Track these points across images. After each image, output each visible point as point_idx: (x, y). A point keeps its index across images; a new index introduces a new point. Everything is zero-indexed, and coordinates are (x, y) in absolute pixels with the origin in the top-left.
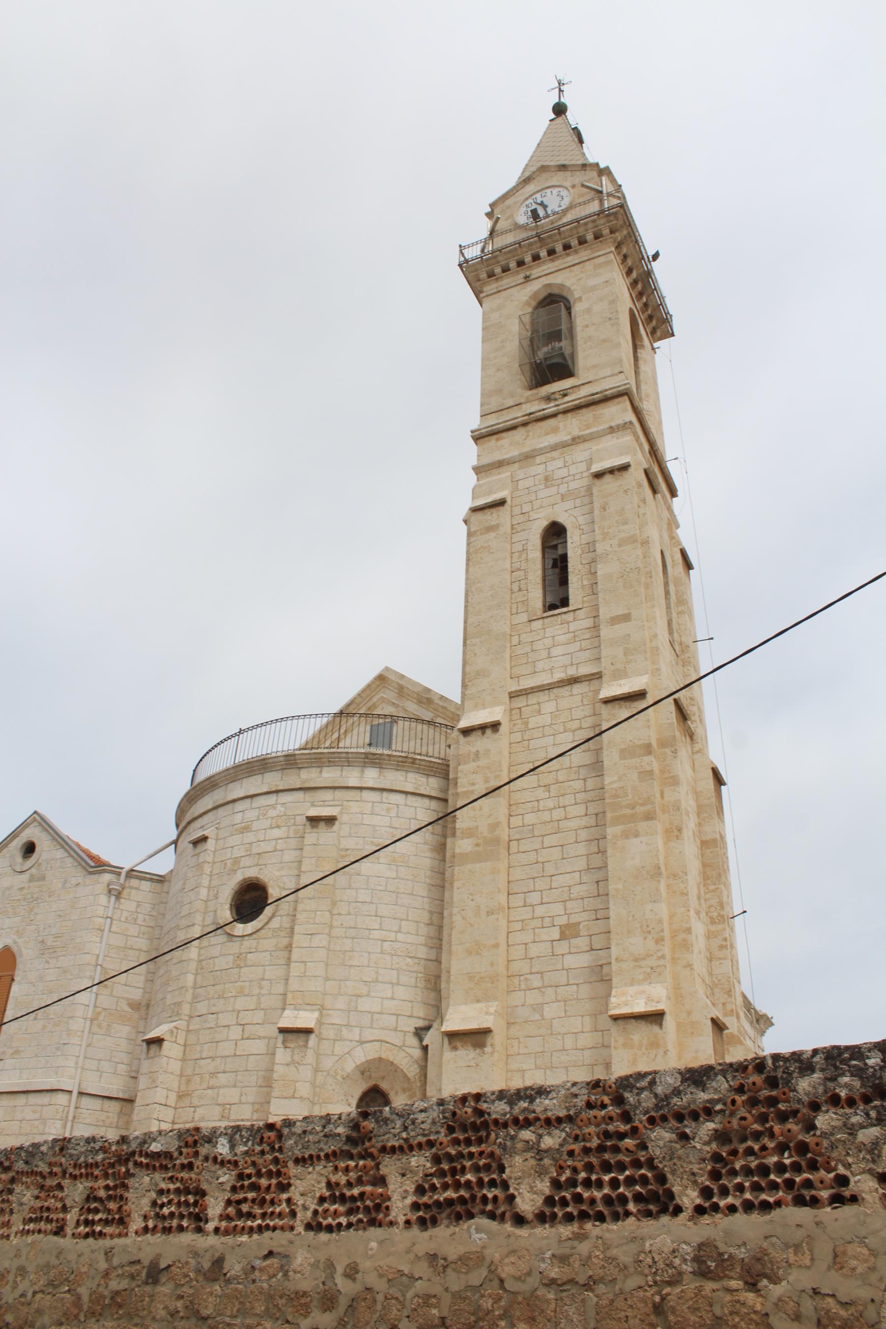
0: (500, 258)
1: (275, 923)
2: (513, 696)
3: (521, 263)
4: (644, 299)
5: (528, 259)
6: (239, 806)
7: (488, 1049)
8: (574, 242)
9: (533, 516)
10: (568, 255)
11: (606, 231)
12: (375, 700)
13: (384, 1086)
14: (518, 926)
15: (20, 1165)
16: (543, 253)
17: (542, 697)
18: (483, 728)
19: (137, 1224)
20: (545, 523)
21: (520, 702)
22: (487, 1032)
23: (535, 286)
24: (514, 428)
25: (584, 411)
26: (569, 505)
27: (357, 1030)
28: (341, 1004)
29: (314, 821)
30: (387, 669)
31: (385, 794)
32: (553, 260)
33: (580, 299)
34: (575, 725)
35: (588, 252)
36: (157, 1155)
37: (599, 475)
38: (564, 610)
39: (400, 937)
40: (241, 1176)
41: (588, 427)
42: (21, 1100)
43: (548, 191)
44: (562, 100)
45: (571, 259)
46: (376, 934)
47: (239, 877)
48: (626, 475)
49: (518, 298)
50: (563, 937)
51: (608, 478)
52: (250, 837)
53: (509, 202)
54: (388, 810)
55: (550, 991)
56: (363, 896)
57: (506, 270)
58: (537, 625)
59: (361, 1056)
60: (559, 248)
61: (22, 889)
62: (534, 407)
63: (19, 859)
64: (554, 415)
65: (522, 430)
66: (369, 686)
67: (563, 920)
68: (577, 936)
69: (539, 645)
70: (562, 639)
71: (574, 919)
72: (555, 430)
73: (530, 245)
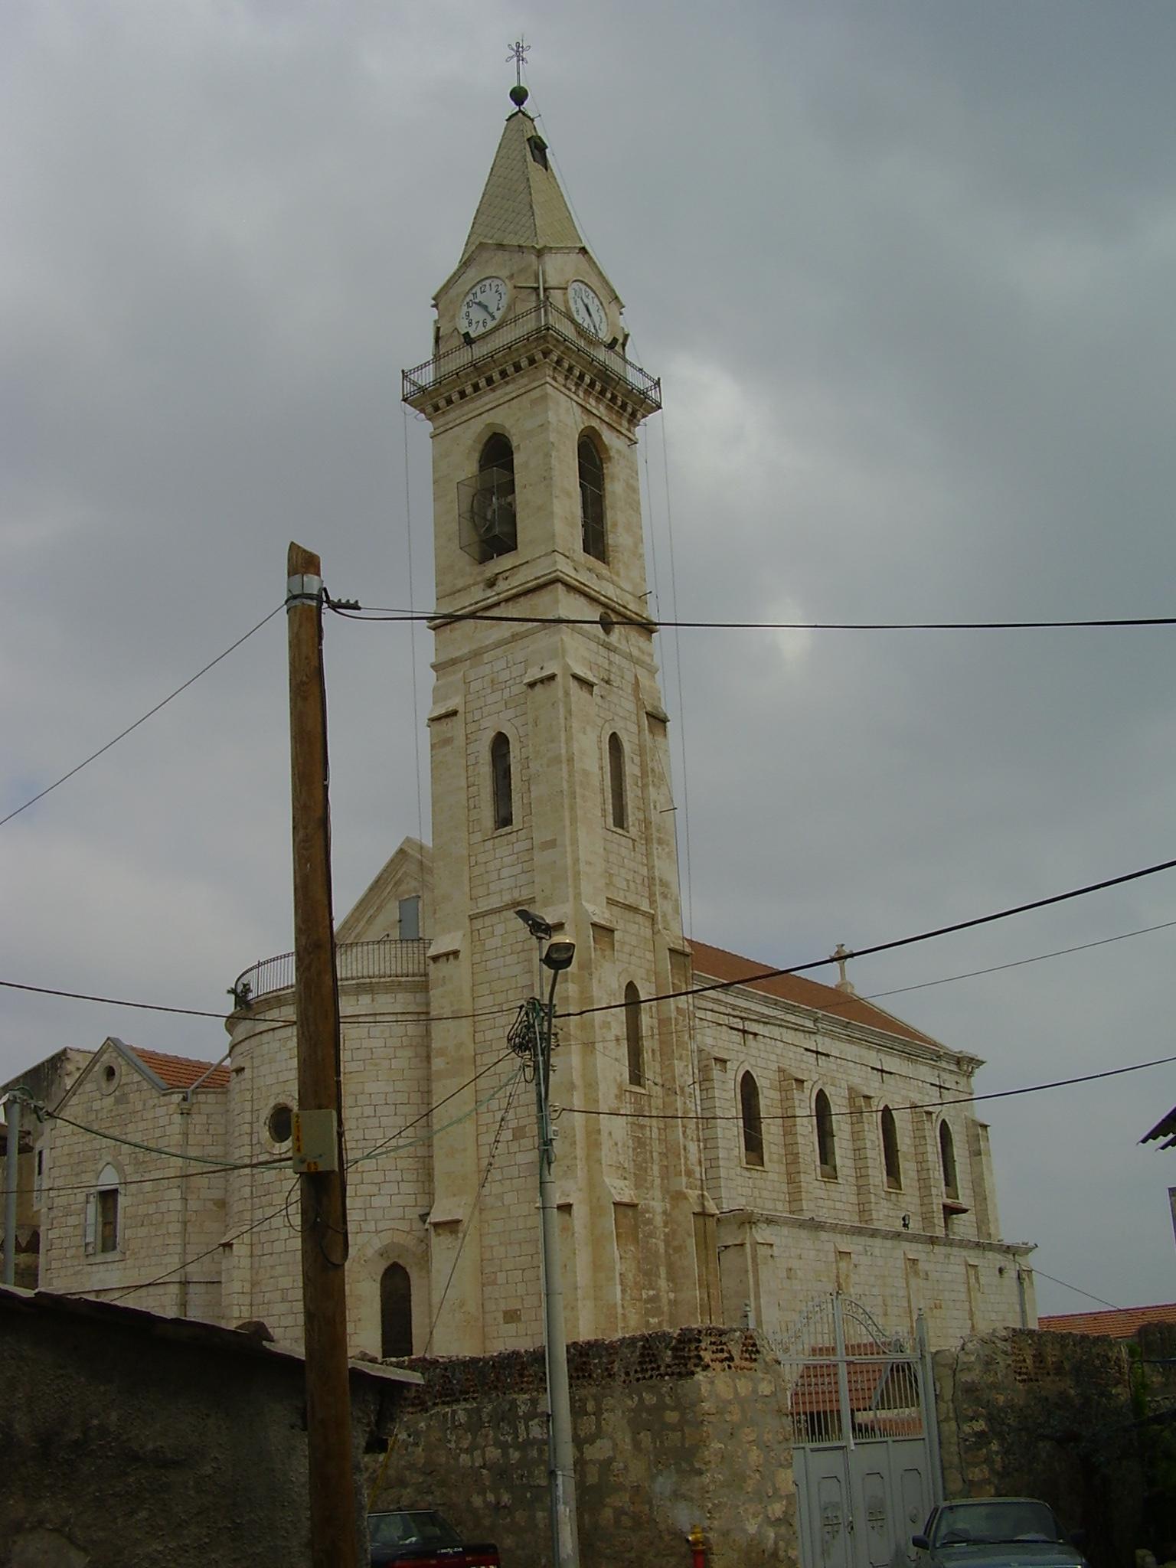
2: (472, 918)
3: (463, 394)
5: (469, 390)
6: (265, 1037)
8: (510, 370)
9: (485, 724)
10: (507, 383)
11: (539, 356)
12: (399, 875)
13: (401, 1262)
14: (484, 1129)
16: (482, 383)
17: (495, 918)
18: (447, 955)
21: (478, 924)
22: (458, 1222)
25: (522, 599)
26: (510, 713)
30: (408, 840)
32: (493, 390)
34: (519, 947)
35: (525, 381)
37: (532, 685)
38: (507, 829)
43: (487, 282)
48: (553, 684)
49: (469, 435)
51: (539, 686)
53: (452, 292)
59: (377, 1243)
60: (496, 376)
63: (104, 1085)
66: (392, 861)
70: (507, 860)
71: (522, 1123)
73: (467, 374)
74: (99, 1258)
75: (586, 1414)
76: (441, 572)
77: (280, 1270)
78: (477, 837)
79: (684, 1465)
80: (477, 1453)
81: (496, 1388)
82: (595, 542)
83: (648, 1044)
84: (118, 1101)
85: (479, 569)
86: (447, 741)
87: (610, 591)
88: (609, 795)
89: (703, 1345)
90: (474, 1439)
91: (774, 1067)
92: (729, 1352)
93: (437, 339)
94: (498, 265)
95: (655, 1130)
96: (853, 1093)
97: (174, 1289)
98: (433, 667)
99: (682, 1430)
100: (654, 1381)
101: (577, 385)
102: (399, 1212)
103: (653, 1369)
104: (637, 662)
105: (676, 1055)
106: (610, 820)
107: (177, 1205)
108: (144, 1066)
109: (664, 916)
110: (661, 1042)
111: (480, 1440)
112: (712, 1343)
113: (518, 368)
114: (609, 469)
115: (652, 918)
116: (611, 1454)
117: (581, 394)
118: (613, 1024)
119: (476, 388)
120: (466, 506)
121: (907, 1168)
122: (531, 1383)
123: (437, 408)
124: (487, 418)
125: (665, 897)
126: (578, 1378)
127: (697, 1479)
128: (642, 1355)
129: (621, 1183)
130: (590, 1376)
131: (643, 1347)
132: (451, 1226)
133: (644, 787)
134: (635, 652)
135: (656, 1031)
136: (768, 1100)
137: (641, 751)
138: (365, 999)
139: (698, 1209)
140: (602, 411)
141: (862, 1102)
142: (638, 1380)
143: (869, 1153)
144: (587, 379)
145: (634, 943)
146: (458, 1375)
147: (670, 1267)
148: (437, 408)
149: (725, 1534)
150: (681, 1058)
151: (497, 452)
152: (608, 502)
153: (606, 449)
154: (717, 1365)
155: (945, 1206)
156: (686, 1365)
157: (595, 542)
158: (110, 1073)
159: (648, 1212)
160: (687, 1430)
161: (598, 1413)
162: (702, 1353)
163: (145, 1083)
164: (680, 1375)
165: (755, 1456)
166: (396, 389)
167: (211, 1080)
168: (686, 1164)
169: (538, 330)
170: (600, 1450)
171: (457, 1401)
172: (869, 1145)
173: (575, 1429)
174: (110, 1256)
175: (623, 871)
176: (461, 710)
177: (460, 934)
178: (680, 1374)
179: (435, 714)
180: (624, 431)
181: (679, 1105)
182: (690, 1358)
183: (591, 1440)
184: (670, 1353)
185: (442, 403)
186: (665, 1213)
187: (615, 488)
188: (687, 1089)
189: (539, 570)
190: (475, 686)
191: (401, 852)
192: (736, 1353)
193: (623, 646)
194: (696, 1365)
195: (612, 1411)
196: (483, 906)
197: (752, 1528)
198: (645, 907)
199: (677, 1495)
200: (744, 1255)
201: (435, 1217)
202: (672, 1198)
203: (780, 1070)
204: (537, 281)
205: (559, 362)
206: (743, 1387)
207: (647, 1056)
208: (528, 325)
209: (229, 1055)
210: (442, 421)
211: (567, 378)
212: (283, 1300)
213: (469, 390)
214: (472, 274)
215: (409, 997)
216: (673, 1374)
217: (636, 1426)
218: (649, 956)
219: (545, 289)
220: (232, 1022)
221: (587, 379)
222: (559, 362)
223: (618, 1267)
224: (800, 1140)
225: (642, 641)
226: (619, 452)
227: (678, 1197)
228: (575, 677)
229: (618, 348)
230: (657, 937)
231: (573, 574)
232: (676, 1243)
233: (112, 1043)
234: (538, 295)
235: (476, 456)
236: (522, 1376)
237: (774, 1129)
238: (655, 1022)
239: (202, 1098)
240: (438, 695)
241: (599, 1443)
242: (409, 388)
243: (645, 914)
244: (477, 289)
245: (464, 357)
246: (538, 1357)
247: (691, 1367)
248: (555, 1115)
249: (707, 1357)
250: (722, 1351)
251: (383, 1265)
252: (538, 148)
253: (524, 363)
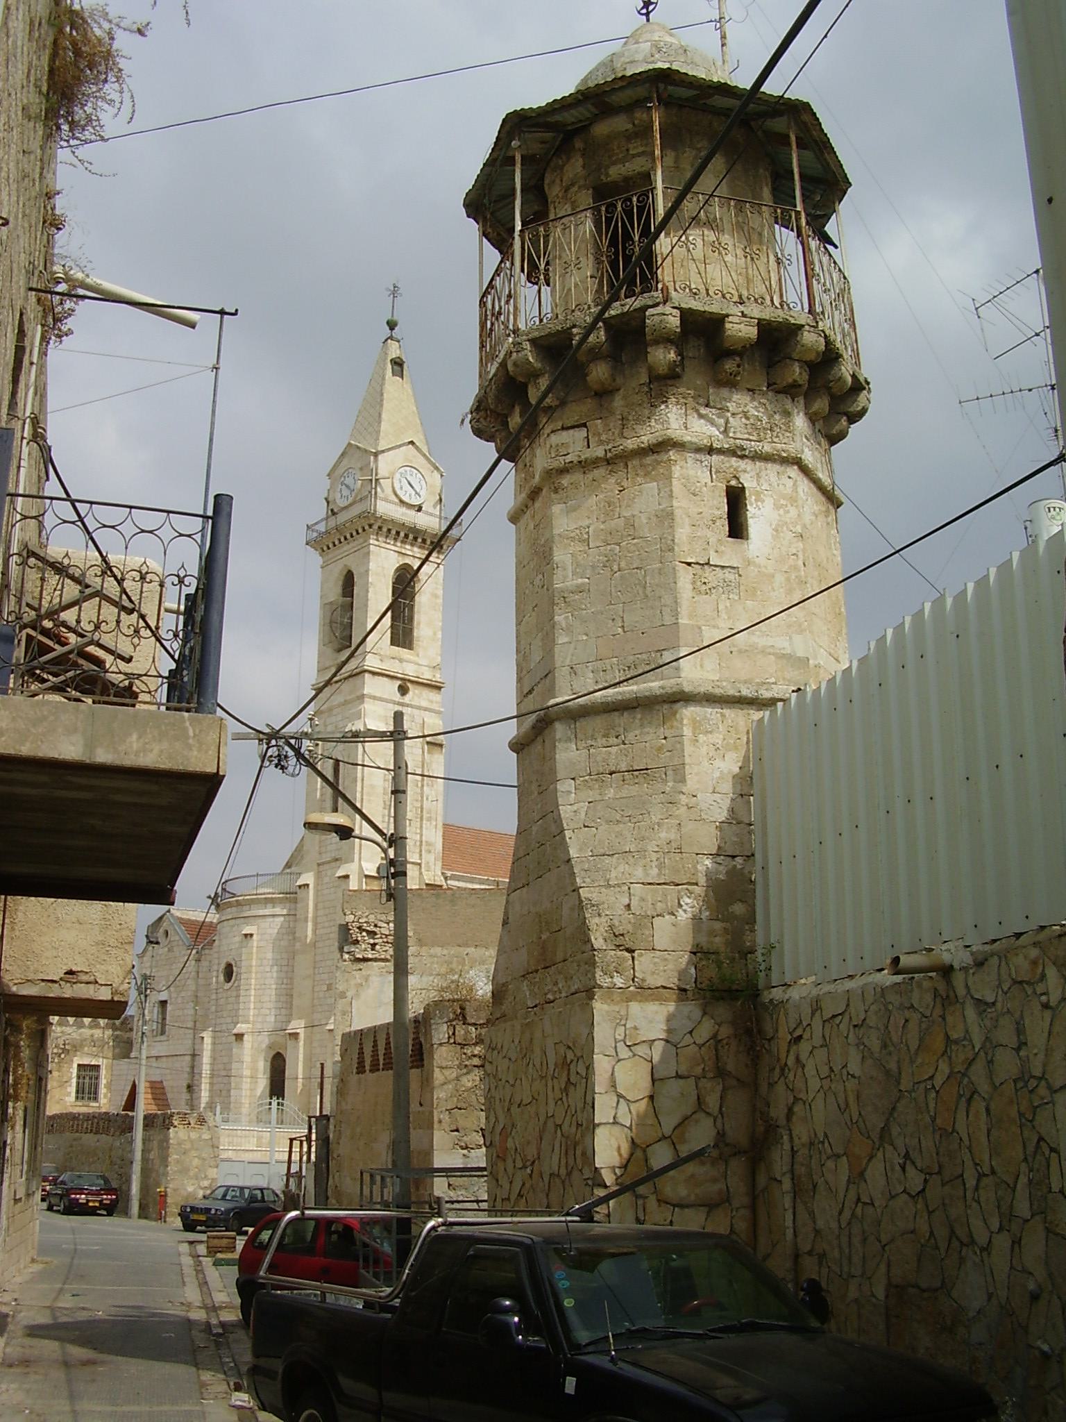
74: (158, 1038)
97: (188, 1058)
101: (395, 539)
107: (192, 1012)
144: (402, 534)
149: (175, 1190)
165: (196, 1162)
174: (163, 1038)
197: (190, 1189)
206: (194, 1135)
221: (402, 534)
235: (341, 583)
249: (176, 1123)
251: (274, 1053)
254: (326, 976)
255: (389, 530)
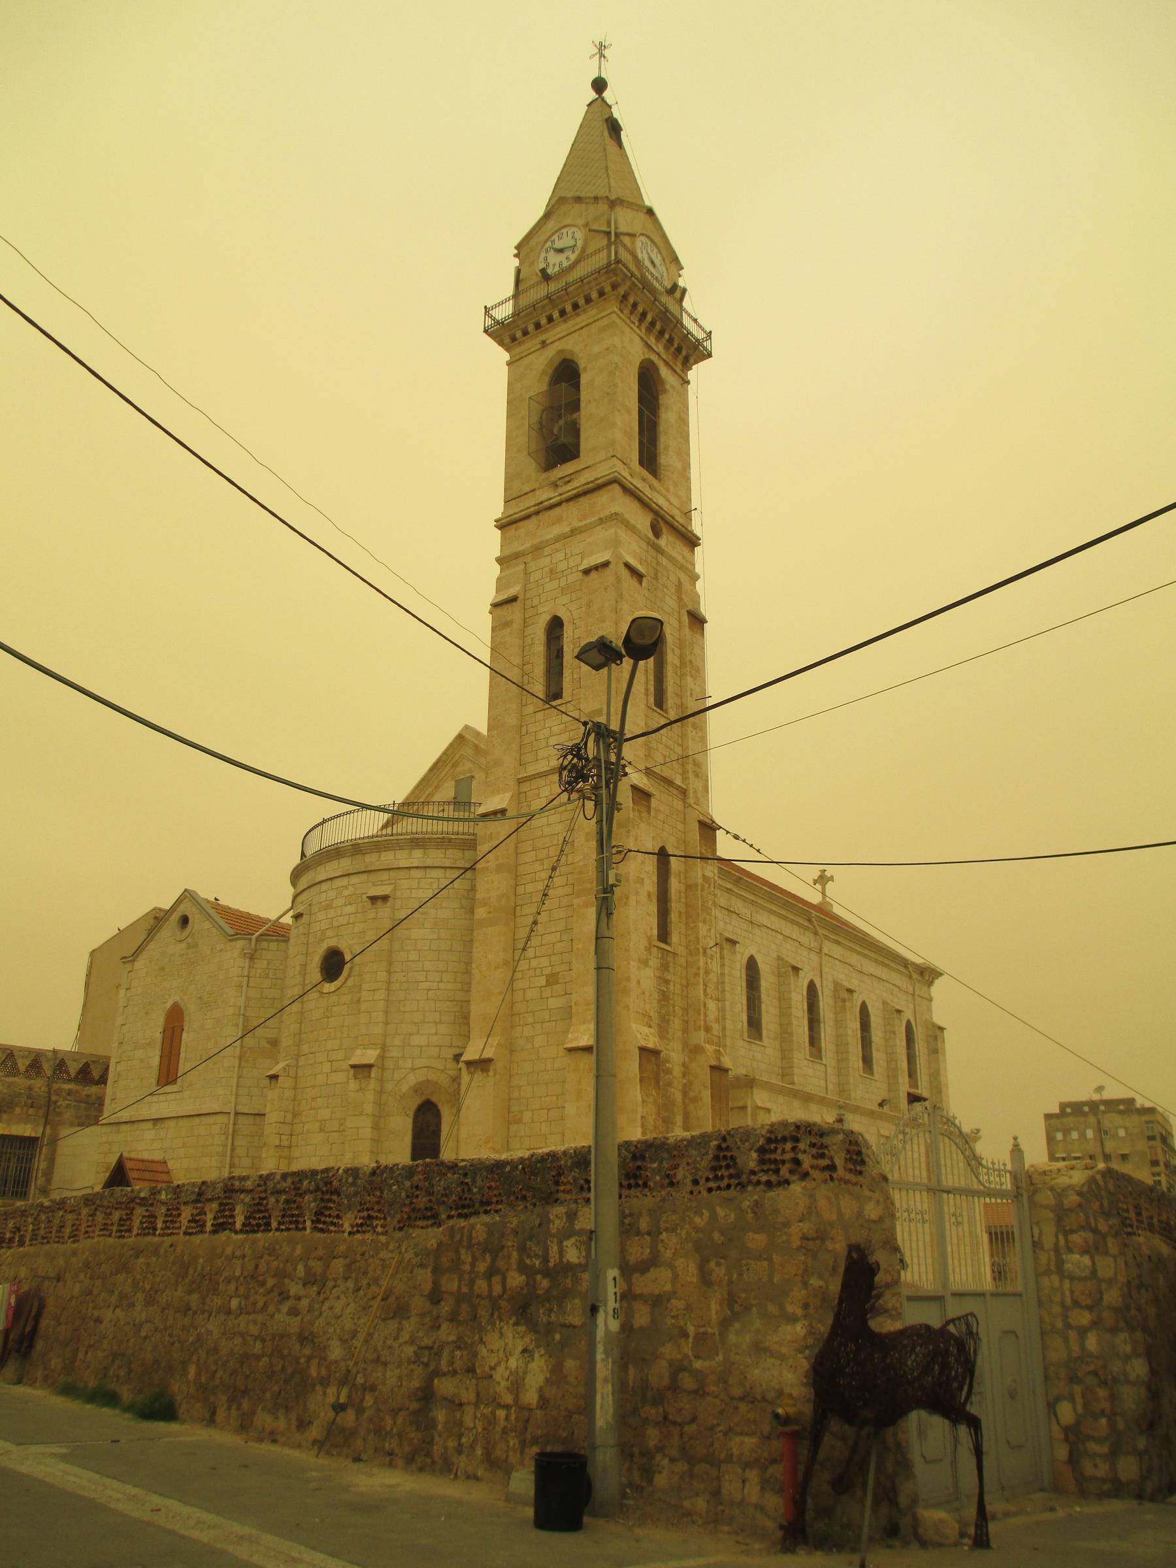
0: (519, 322)
1: (350, 982)
2: (520, 781)
3: (538, 326)
4: (667, 336)
5: (543, 321)
6: (324, 886)
7: (491, 1073)
8: (582, 302)
10: (578, 315)
11: (608, 289)
13: (434, 1099)
15: (98, 1202)
16: (556, 315)
18: (495, 813)
19: (135, 1232)
20: (548, 617)
21: (525, 787)
23: (550, 353)
24: (527, 517)
26: (565, 599)
27: (410, 1061)
28: (398, 1041)
29: (373, 899)
30: (466, 727)
31: (428, 871)
32: (565, 321)
33: (585, 368)
35: (594, 312)
36: (143, 1199)
37: (587, 572)
39: (442, 985)
40: (168, 1210)
41: (585, 517)
42: (197, 1120)
43: (564, 231)
44: (603, 76)
45: (582, 320)
46: (423, 986)
47: (324, 946)
49: (541, 361)
50: (548, 984)
52: (331, 913)
53: (533, 243)
54: (431, 884)
55: (538, 1026)
56: (413, 956)
57: (525, 333)
58: (540, 716)
59: (412, 1080)
60: (569, 308)
61: (182, 955)
62: (545, 495)
64: (559, 504)
65: (534, 519)
66: (451, 745)
67: (547, 971)
68: (557, 983)
69: (541, 736)
70: (556, 729)
71: (556, 970)
72: (559, 520)
73: (543, 307)
75: (638, 1233)
76: (509, 479)
77: (320, 1102)
78: (530, 709)
79: (771, 1308)
80: (496, 1279)
81: (524, 1198)
82: (649, 458)
83: (676, 907)
84: (189, 947)
85: (544, 475)
86: (507, 624)
87: (661, 502)
88: (651, 677)
89: (802, 1146)
90: (494, 1260)
91: (774, 955)
92: (831, 1158)
93: (518, 282)
94: (576, 214)
95: (678, 986)
96: (837, 985)
98: (499, 560)
99: (769, 1259)
100: (732, 1193)
102: (435, 1051)
103: (731, 1176)
104: (682, 568)
105: (701, 918)
106: (652, 699)
108: (217, 917)
109: (695, 792)
110: (687, 906)
111: (501, 1264)
112: (813, 1145)
113: (588, 300)
114: (664, 400)
115: (684, 793)
116: (668, 1287)
117: (643, 330)
118: (647, 881)
119: (550, 319)
120: (535, 419)
121: (878, 1056)
122: (569, 1192)
123: (514, 339)
124: (558, 346)
125: (697, 775)
126: (629, 1187)
127: (789, 1328)
128: (716, 1158)
129: (646, 1030)
130: (645, 1185)
131: (719, 1148)
132: (482, 1065)
133: (682, 676)
134: (680, 559)
135: (683, 895)
136: (767, 982)
137: (681, 644)
138: (418, 853)
139: (714, 1063)
140: (660, 348)
141: (846, 995)
142: (710, 1190)
143: (850, 1040)
145: (667, 812)
146: (479, 1182)
147: (686, 1116)
148: (514, 339)
150: (704, 922)
151: (566, 374)
152: (662, 427)
153: (662, 382)
154: (815, 1174)
155: (909, 1094)
156: (777, 1171)
157: (649, 458)
158: (185, 921)
159: (668, 1061)
160: (776, 1258)
161: (654, 1232)
162: (801, 1157)
163: (214, 930)
164: (769, 1184)
166: (479, 322)
167: (276, 933)
168: (705, 1021)
169: (609, 265)
170: (657, 1281)
171: (477, 1213)
172: (850, 1032)
173: (623, 1251)
175: (660, 747)
176: (521, 597)
177: (508, 795)
178: (769, 1184)
179: (499, 599)
180: (678, 371)
181: (701, 964)
182: (783, 1162)
183: (644, 1267)
184: (754, 1155)
185: (519, 334)
186: (684, 1065)
187: (667, 417)
188: (709, 951)
189: (601, 472)
190: (535, 576)
191: (460, 738)
192: (839, 1161)
193: (669, 550)
194: (791, 1172)
195: (674, 1230)
196: (531, 770)
198: (678, 781)
199: (759, 1349)
200: (746, 1114)
201: (468, 1056)
202: (691, 1051)
203: (779, 958)
204: (609, 225)
205: (625, 297)
206: (848, 1206)
207: (674, 917)
208: (600, 260)
209: (292, 908)
210: (518, 350)
211: (632, 312)
212: (322, 1130)
213: (543, 321)
214: (551, 225)
215: (458, 854)
216: (759, 1183)
217: (705, 1252)
218: (680, 826)
219: (616, 235)
220: (296, 875)
221: (649, 318)
222: (625, 297)
223: (640, 1109)
224: (794, 1021)
225: (685, 551)
226: (673, 387)
227: (695, 1051)
228: (627, 566)
229: (678, 294)
230: (687, 810)
231: (629, 478)
232: (692, 1094)
233: (187, 896)
234: (609, 239)
235: (547, 379)
236: (557, 1183)
237: (771, 1009)
238: (683, 887)
239: (264, 945)
240: (501, 584)
241: (653, 1273)
242: (489, 322)
243: (678, 788)
244: (555, 237)
245: (541, 291)
246: (581, 1159)
247: (784, 1171)
248: (616, 858)
249: (807, 1161)
250: (822, 1156)
251: (416, 1102)
252: (614, 128)
253: (594, 295)
254: (544, 962)
255: (635, 305)
